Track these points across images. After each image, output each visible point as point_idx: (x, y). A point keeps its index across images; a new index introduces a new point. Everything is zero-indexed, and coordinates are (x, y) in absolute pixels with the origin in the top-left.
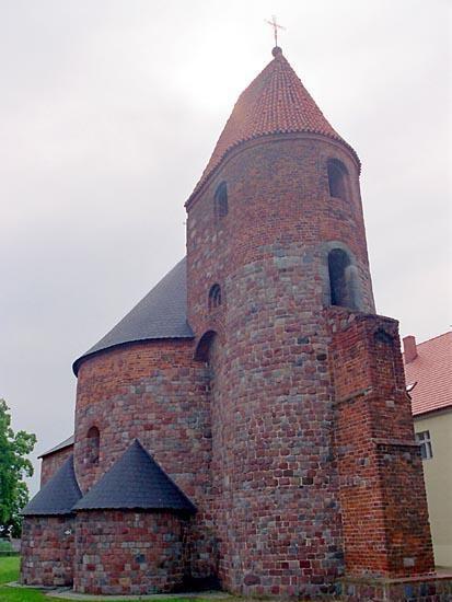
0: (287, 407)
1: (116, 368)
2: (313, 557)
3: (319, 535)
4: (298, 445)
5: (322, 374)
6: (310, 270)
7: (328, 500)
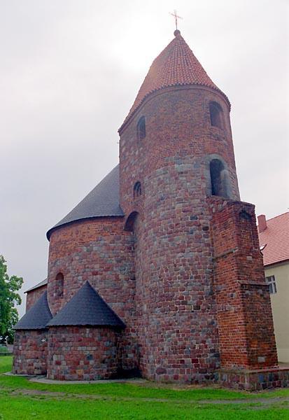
0: (184, 260)
1: (74, 235)
2: (200, 356)
3: (204, 342)
4: (191, 285)
5: (206, 239)
6: (198, 173)
7: (210, 320)
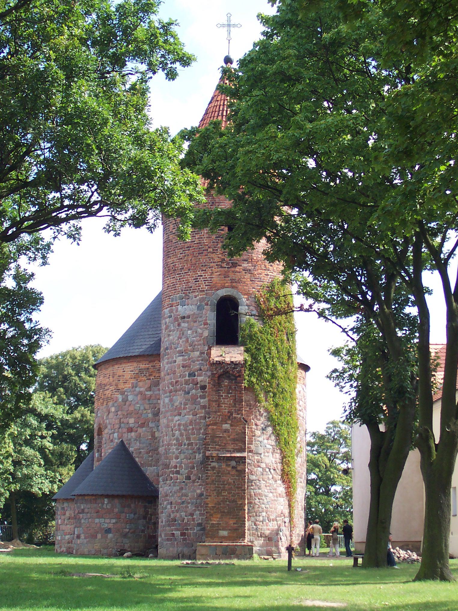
0: (179, 425)
2: (187, 529)
3: (192, 515)
4: (184, 453)
5: (202, 401)
6: (201, 317)
7: (199, 491)
